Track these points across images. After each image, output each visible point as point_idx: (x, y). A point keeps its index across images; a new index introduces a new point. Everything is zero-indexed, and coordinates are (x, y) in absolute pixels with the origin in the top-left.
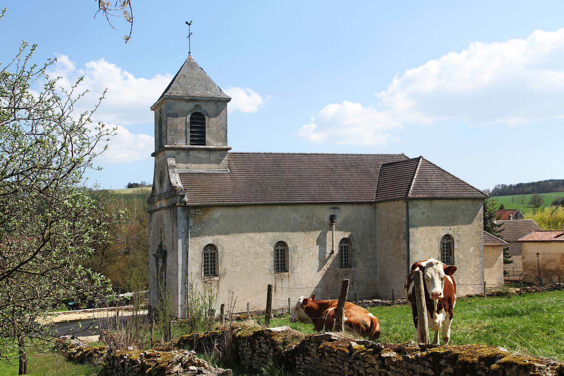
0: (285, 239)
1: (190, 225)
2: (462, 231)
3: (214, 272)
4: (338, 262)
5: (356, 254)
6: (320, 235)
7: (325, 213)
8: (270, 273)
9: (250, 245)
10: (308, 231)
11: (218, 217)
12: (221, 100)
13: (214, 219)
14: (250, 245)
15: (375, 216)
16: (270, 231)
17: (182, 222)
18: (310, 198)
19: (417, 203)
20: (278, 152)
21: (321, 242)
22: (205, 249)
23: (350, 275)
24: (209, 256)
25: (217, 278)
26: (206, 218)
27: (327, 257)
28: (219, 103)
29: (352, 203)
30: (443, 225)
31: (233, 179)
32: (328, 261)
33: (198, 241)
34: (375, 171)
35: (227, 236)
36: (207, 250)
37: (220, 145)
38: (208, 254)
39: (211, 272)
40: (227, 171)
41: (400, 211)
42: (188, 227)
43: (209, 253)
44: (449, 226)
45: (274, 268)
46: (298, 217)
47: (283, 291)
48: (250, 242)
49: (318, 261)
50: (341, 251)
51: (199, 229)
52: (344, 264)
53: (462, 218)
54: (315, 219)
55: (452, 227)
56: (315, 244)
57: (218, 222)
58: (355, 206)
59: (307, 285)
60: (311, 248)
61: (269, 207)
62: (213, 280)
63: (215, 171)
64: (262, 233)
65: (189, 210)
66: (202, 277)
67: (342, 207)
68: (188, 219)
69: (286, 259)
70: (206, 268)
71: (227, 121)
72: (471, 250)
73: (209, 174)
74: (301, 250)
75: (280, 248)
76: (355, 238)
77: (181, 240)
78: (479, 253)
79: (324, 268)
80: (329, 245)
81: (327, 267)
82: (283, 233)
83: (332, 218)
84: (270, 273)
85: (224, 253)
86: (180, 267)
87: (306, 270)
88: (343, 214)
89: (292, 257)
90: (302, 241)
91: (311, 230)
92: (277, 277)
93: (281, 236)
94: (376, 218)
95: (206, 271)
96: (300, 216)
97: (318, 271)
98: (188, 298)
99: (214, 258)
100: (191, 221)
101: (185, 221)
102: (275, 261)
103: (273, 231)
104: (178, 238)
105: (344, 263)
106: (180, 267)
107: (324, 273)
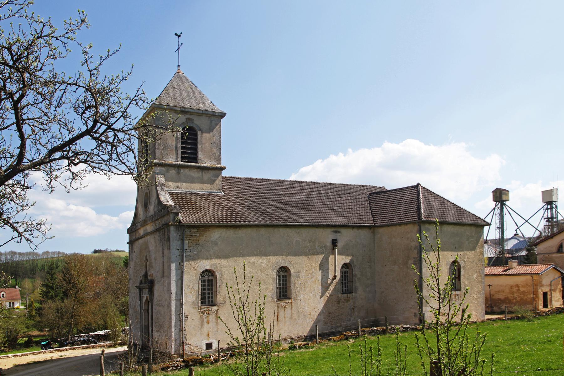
0: (288, 264)
1: (185, 248)
2: (467, 257)
3: (212, 301)
4: (340, 288)
5: (357, 280)
6: (322, 260)
7: (327, 236)
8: (273, 301)
9: (251, 270)
10: (311, 255)
11: (217, 239)
12: (215, 114)
13: (212, 241)
14: (251, 270)
15: (374, 240)
16: (273, 255)
17: (175, 244)
18: (312, 220)
19: (429, 227)
20: (269, 179)
21: (323, 267)
22: (202, 275)
23: (351, 301)
24: (206, 283)
25: (215, 308)
26: (202, 240)
27: (329, 283)
28: (212, 118)
29: (353, 227)
30: (452, 250)
31: (229, 200)
32: (331, 287)
33: (194, 265)
34: (364, 198)
35: (226, 260)
36: (203, 276)
37: (213, 164)
38: (204, 281)
39: (209, 301)
40: (221, 192)
41: (409, 236)
42: (182, 250)
43: (206, 279)
44: (456, 252)
45: (277, 295)
46: (301, 240)
47: (286, 320)
48: (251, 267)
49: (320, 287)
50: (342, 276)
51: (196, 253)
52: (344, 290)
53: (467, 244)
54: (317, 243)
55: (459, 253)
56: (318, 269)
57: (216, 244)
58: (355, 230)
59: (310, 313)
60: (313, 273)
61: (271, 229)
62: (212, 310)
63: (208, 192)
64: (264, 258)
65: (184, 230)
66: (198, 307)
67: (343, 231)
68: (182, 240)
69: (288, 285)
70: (203, 296)
71: (220, 138)
72: (475, 276)
73: (202, 195)
74: (304, 276)
75: (282, 274)
76: (355, 263)
77: (174, 264)
78: (481, 279)
79: (326, 295)
80: (331, 270)
81: (329, 294)
82: (286, 258)
83: (334, 243)
84: (273, 301)
85: (224, 279)
86: (174, 296)
87: (308, 297)
88: (345, 237)
89: (295, 283)
90: (305, 266)
91: (313, 254)
92: (280, 305)
93: (283, 261)
94: (374, 243)
95: (203, 300)
96: (302, 240)
97: (321, 298)
98: (183, 330)
99: (212, 285)
100: (186, 242)
101: (179, 243)
102: (277, 288)
103: (275, 254)
104: (170, 262)
105: (344, 289)
106: (174, 296)
107: (327, 299)
